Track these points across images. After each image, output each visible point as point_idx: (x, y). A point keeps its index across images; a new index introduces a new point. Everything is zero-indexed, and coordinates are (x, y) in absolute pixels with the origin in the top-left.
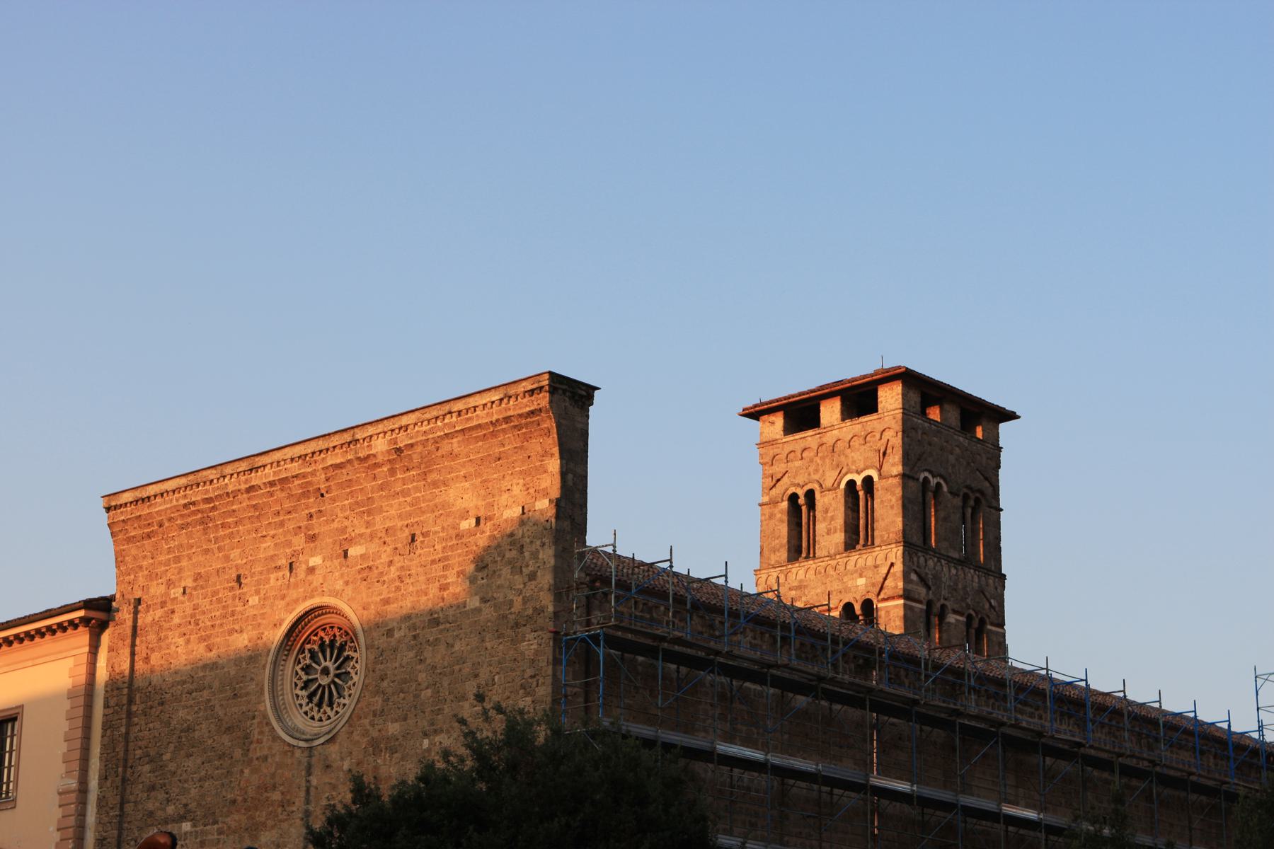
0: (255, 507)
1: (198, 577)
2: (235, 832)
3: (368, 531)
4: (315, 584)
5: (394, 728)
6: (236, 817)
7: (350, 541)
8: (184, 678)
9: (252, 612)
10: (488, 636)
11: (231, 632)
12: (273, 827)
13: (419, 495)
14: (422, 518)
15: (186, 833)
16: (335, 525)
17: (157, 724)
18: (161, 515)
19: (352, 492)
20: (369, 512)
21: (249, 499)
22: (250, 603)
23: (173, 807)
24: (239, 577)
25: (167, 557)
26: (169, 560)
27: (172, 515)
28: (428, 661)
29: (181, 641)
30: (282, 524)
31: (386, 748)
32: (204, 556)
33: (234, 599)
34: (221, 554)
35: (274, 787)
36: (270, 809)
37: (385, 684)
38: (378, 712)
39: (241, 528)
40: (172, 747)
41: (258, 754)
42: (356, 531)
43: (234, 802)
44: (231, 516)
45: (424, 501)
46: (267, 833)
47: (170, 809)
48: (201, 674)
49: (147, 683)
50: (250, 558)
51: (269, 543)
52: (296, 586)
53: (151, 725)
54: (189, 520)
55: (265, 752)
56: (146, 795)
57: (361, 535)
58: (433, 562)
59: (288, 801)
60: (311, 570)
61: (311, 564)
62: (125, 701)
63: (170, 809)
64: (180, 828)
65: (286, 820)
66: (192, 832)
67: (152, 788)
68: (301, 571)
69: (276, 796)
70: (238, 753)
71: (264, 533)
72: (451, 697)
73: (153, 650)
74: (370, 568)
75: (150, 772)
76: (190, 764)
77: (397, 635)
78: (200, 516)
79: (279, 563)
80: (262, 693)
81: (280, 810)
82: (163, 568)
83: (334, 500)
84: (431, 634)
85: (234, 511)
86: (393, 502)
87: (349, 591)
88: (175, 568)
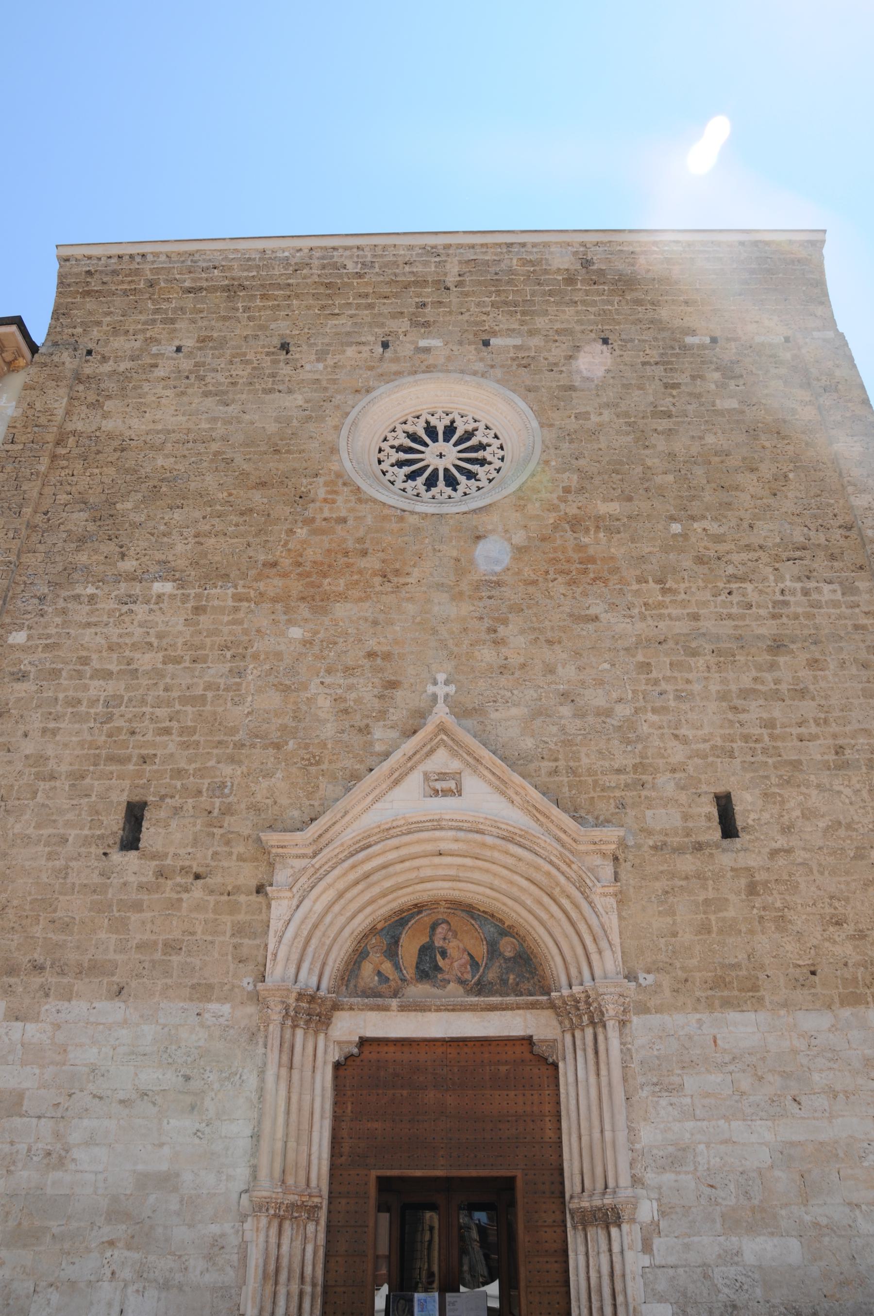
0: (328, 286)
1: (202, 340)
2: (275, 600)
3: (526, 328)
4: (431, 361)
5: (604, 508)
6: (278, 582)
7: (494, 334)
8: (170, 427)
9: (310, 376)
10: (763, 437)
11: (271, 391)
12: (361, 600)
13: (610, 307)
14: (617, 327)
15: (159, 596)
16: (466, 317)
17: (111, 471)
18: (158, 274)
19: (499, 291)
20: (524, 313)
21: (319, 276)
22: (308, 367)
23: (135, 563)
24: (285, 347)
25: (151, 317)
26: (154, 321)
27: (178, 277)
28: (660, 448)
29: (168, 392)
30: (371, 306)
31: (598, 527)
32: (221, 323)
33: (275, 362)
34: (251, 324)
35: (364, 553)
36: (355, 577)
37: (582, 462)
38: (573, 489)
39: (295, 302)
40: (139, 496)
41: (326, 514)
42: (501, 326)
43: (274, 565)
44: (281, 289)
45: (618, 314)
46: (349, 606)
47: (128, 565)
48: (205, 425)
49: (94, 428)
50: (306, 330)
51: (342, 320)
52: (396, 360)
53: (97, 471)
54: (205, 284)
55: (343, 514)
56: (74, 546)
57: (514, 330)
58: (644, 364)
59: (397, 570)
60: (427, 350)
61: (423, 343)
62: (50, 438)
63: (128, 565)
64: (150, 588)
65: (392, 592)
66: (172, 597)
67: (82, 540)
68: (404, 348)
69: (372, 563)
70: (282, 510)
71: (337, 311)
72: (714, 485)
73: (109, 397)
74: (533, 358)
75: (87, 521)
76: (177, 515)
77: (594, 418)
78: (227, 282)
79: (363, 339)
80: (334, 450)
81: (377, 580)
82: (140, 326)
83: (467, 295)
84: (664, 424)
85: (289, 285)
86: (567, 309)
87: (498, 372)
88: (164, 329)
